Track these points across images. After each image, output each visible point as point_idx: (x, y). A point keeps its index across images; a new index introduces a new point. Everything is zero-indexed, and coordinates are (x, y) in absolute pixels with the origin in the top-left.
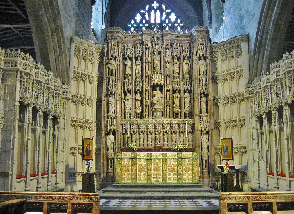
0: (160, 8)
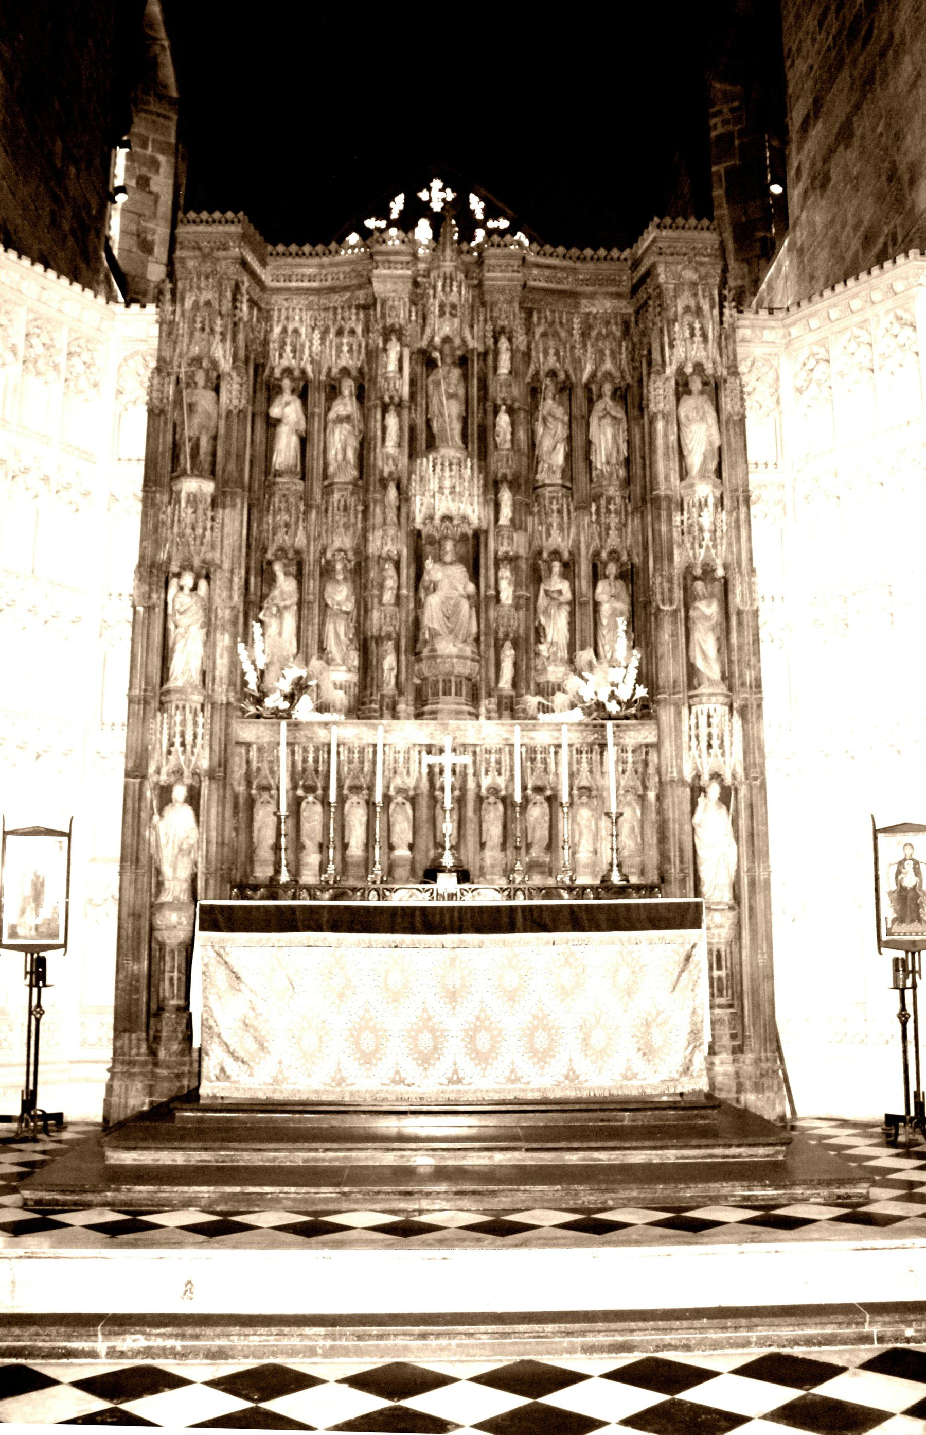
0: (459, 208)
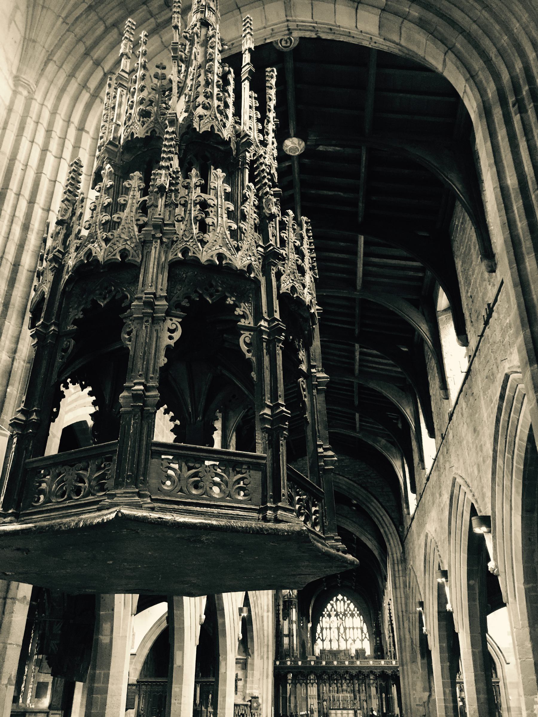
0: (343, 599)
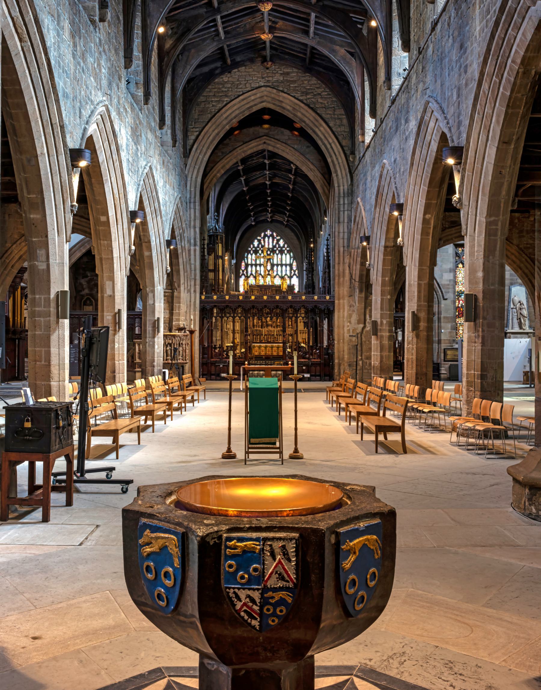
0: (272, 235)
